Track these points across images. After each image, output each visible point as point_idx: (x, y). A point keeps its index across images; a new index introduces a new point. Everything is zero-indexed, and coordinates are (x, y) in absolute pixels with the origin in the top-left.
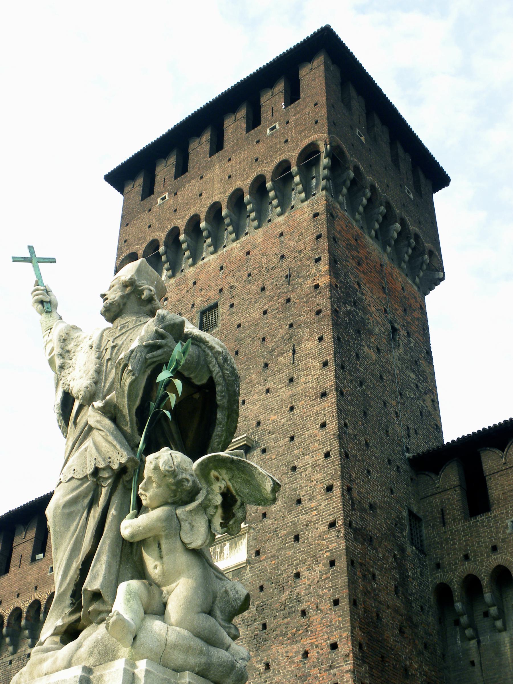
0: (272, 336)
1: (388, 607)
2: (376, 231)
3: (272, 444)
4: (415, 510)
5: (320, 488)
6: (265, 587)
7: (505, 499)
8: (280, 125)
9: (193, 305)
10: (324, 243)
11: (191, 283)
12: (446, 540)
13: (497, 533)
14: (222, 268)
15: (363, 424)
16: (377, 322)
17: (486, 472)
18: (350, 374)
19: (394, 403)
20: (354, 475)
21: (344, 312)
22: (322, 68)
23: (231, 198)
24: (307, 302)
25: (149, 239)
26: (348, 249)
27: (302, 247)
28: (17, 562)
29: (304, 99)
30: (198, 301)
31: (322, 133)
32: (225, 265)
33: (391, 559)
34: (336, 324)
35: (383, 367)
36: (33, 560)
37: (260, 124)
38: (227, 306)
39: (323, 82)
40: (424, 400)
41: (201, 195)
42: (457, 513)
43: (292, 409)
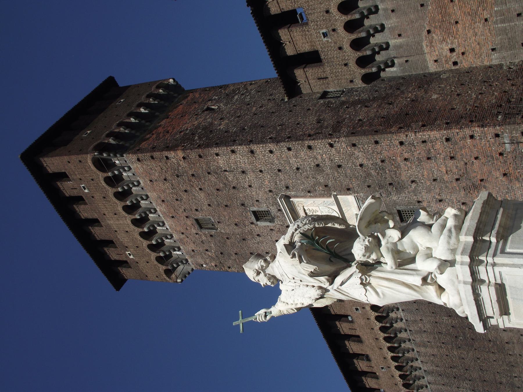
0: (215, 185)
1: (377, 111)
2: (147, 122)
3: (283, 183)
4: (319, 95)
5: (309, 153)
6: (368, 185)
7: (311, 42)
8: (82, 184)
9: (197, 234)
10: (156, 154)
11: (184, 236)
12: (336, 77)
13: (332, 47)
14: (173, 217)
15: (269, 128)
16: (204, 120)
17: (295, 53)
18: (239, 136)
19: (254, 109)
20: (301, 133)
21: (200, 141)
22: (46, 159)
23: (129, 213)
24: (194, 164)
25: (156, 263)
26: (159, 139)
27: (159, 168)
28: (353, 331)
29: (65, 169)
30: (194, 231)
31: (87, 158)
32: (171, 215)
33: (349, 110)
34: (208, 145)
35: (232, 116)
36: (352, 322)
37: (82, 196)
38: (197, 213)
39: (55, 158)
40: (251, 90)
41: (127, 232)
42: (320, 70)
43: (261, 171)
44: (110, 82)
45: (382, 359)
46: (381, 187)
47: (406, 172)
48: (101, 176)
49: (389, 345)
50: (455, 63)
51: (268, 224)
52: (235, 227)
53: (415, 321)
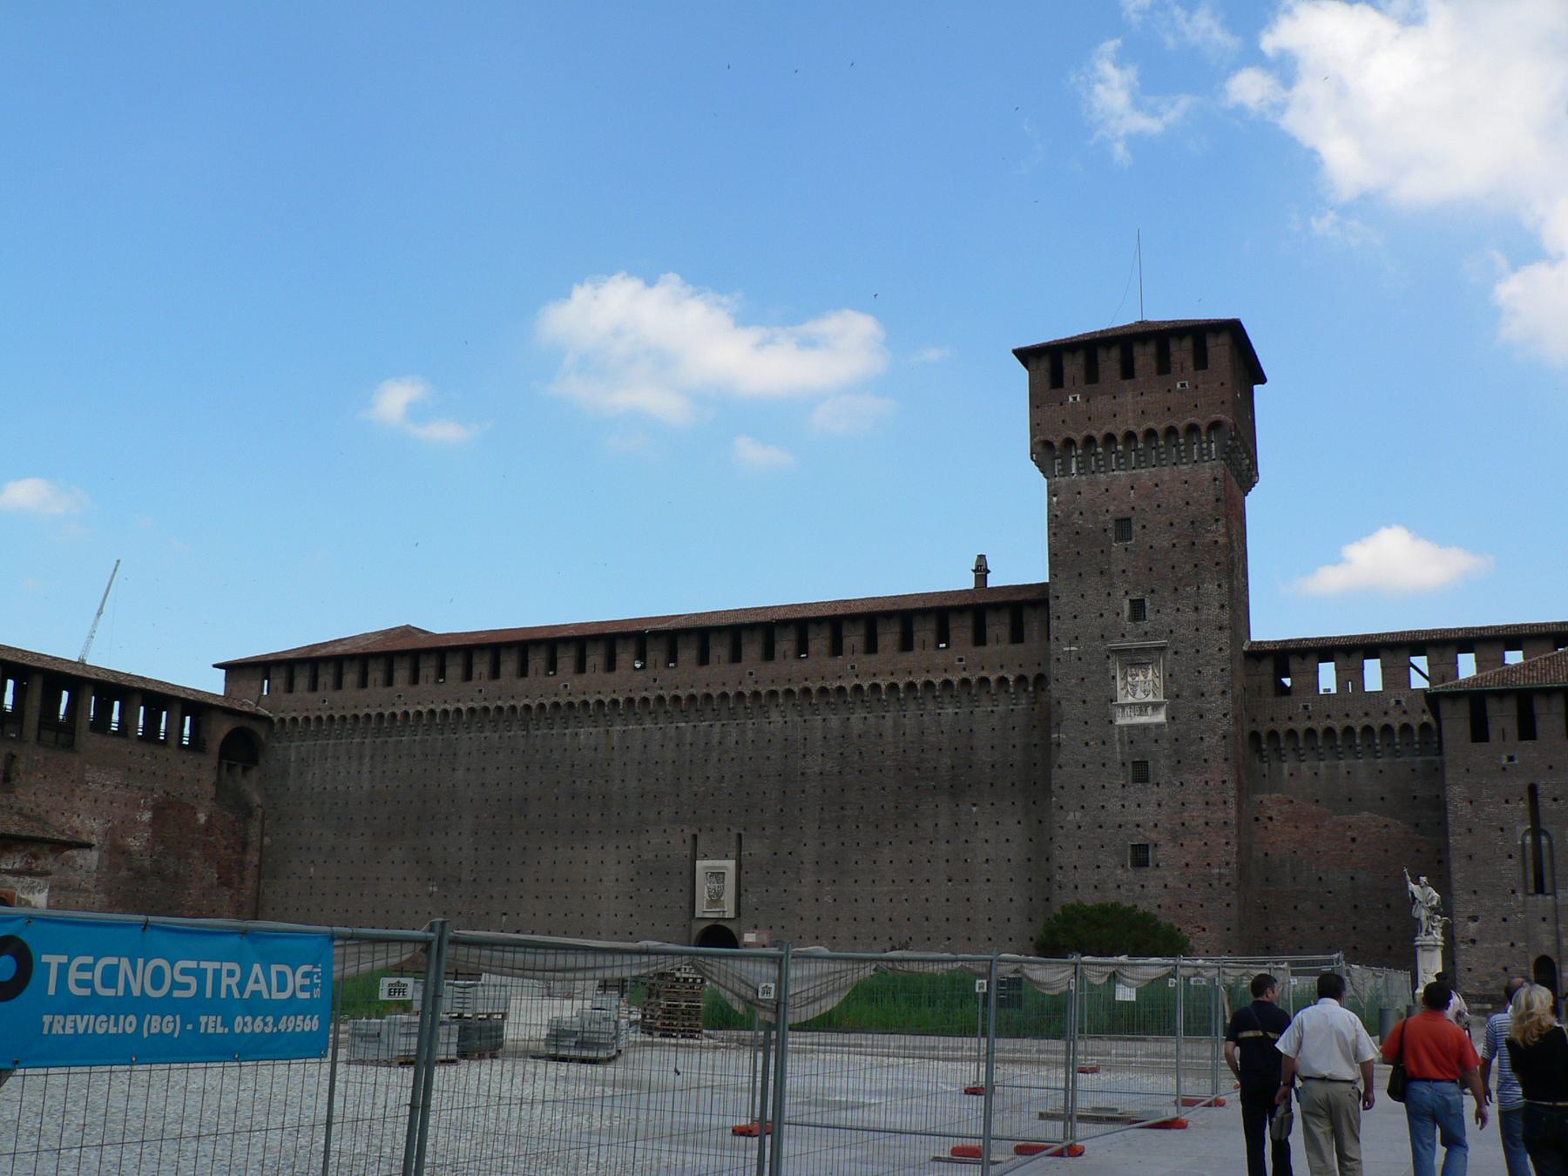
30: (1112, 508)
44: (1263, 380)
45: (872, 671)
49: (901, 686)
50: (1257, 819)
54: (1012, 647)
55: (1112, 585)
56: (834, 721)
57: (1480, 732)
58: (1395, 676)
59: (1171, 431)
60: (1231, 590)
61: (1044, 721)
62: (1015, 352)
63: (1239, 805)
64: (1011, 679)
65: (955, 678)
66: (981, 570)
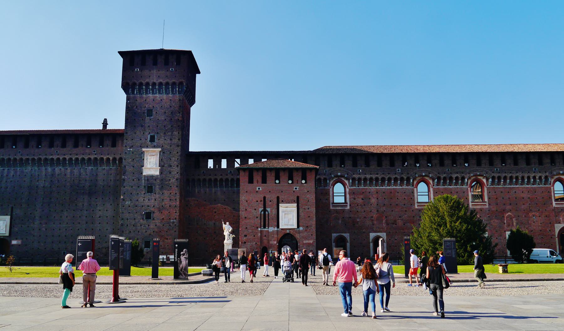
30: (147, 106)
44: (199, 73)
46: (162, 184)
47: (166, 193)
48: (177, 82)
51: (149, 139)
52: (148, 125)
53: (86, 172)
54: (113, 148)
55: (145, 130)
56: (50, 169)
57: (251, 181)
58: (230, 164)
59: (167, 84)
60: (182, 135)
61: (121, 171)
62: (119, 52)
63: (180, 201)
64: (111, 158)
65: (92, 157)
66: (105, 123)
